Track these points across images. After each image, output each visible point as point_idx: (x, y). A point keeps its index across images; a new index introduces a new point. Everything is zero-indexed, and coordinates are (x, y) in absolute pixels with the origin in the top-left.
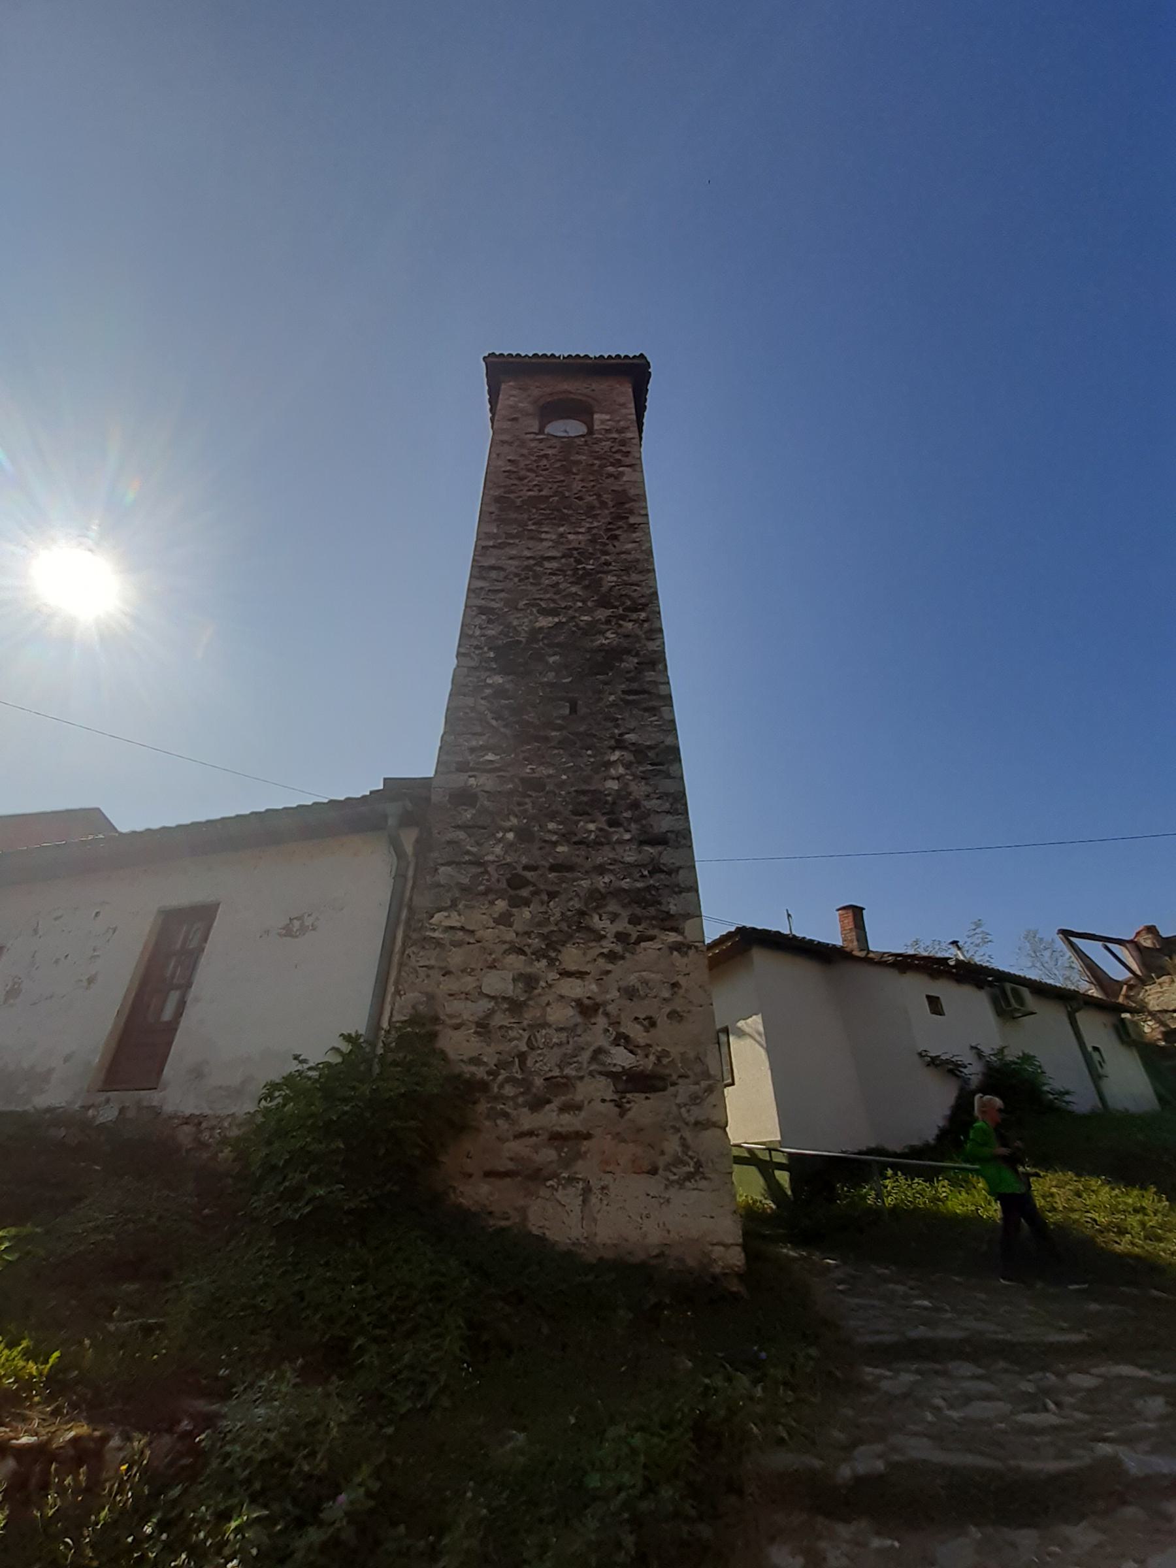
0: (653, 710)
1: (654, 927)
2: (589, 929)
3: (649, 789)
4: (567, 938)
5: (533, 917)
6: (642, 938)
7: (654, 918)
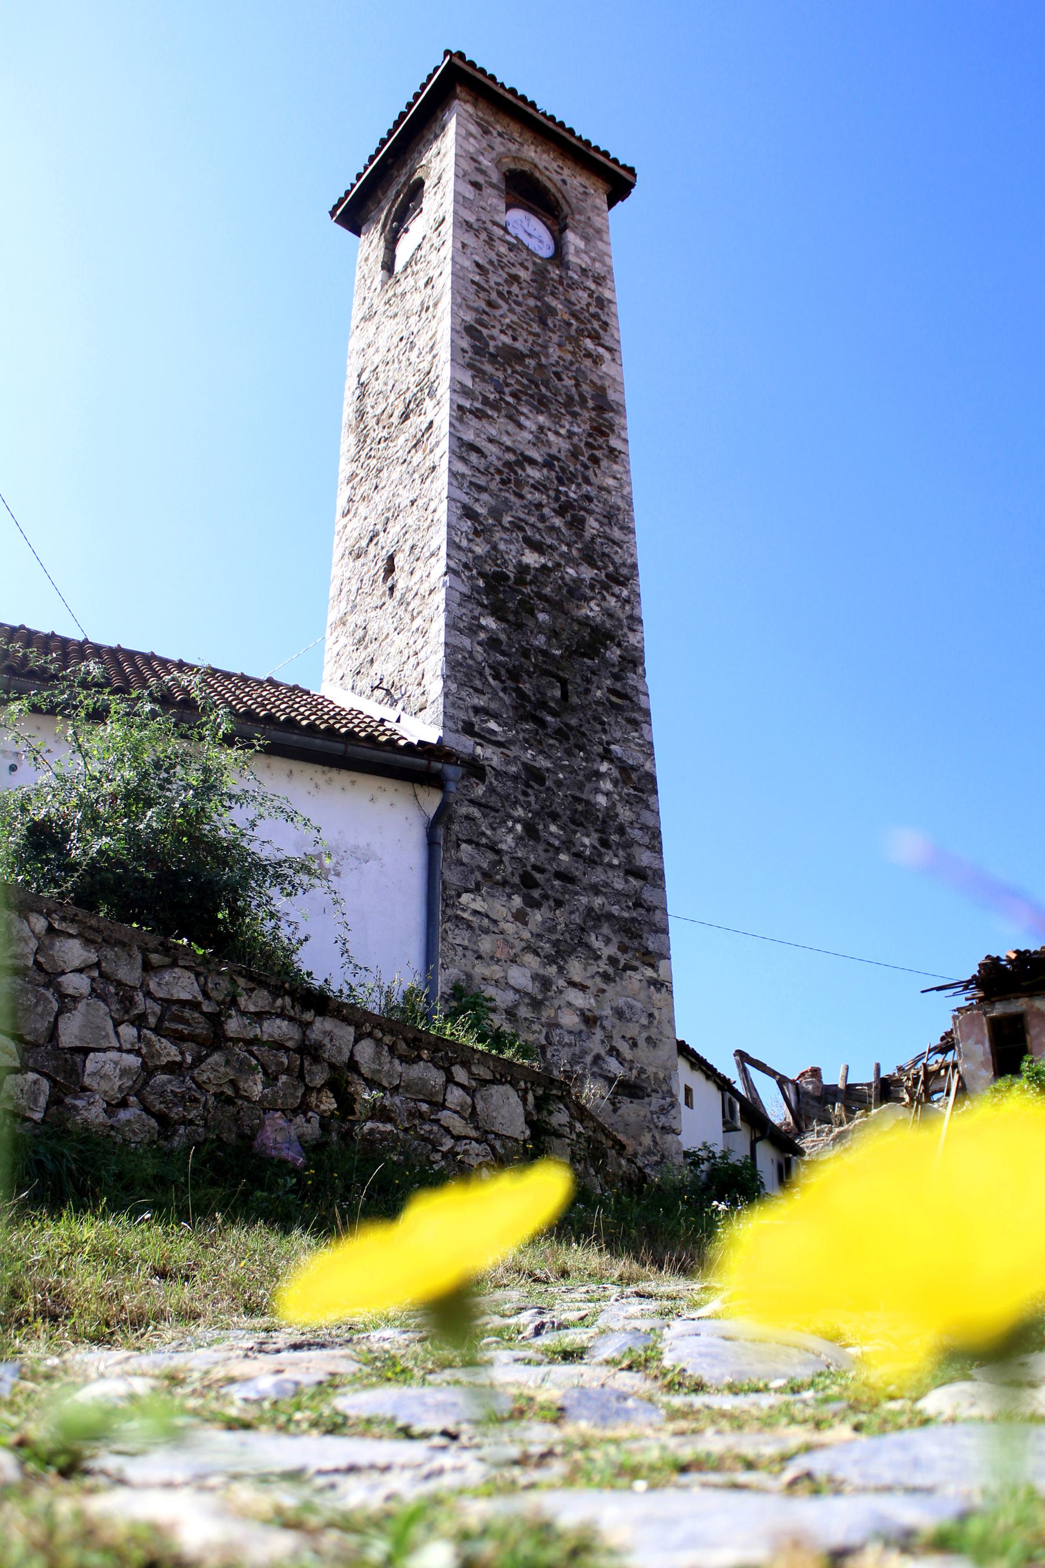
0: (635, 724)
1: (637, 959)
2: (588, 947)
3: (634, 818)
4: (572, 951)
5: (544, 922)
6: (628, 967)
7: (637, 950)
